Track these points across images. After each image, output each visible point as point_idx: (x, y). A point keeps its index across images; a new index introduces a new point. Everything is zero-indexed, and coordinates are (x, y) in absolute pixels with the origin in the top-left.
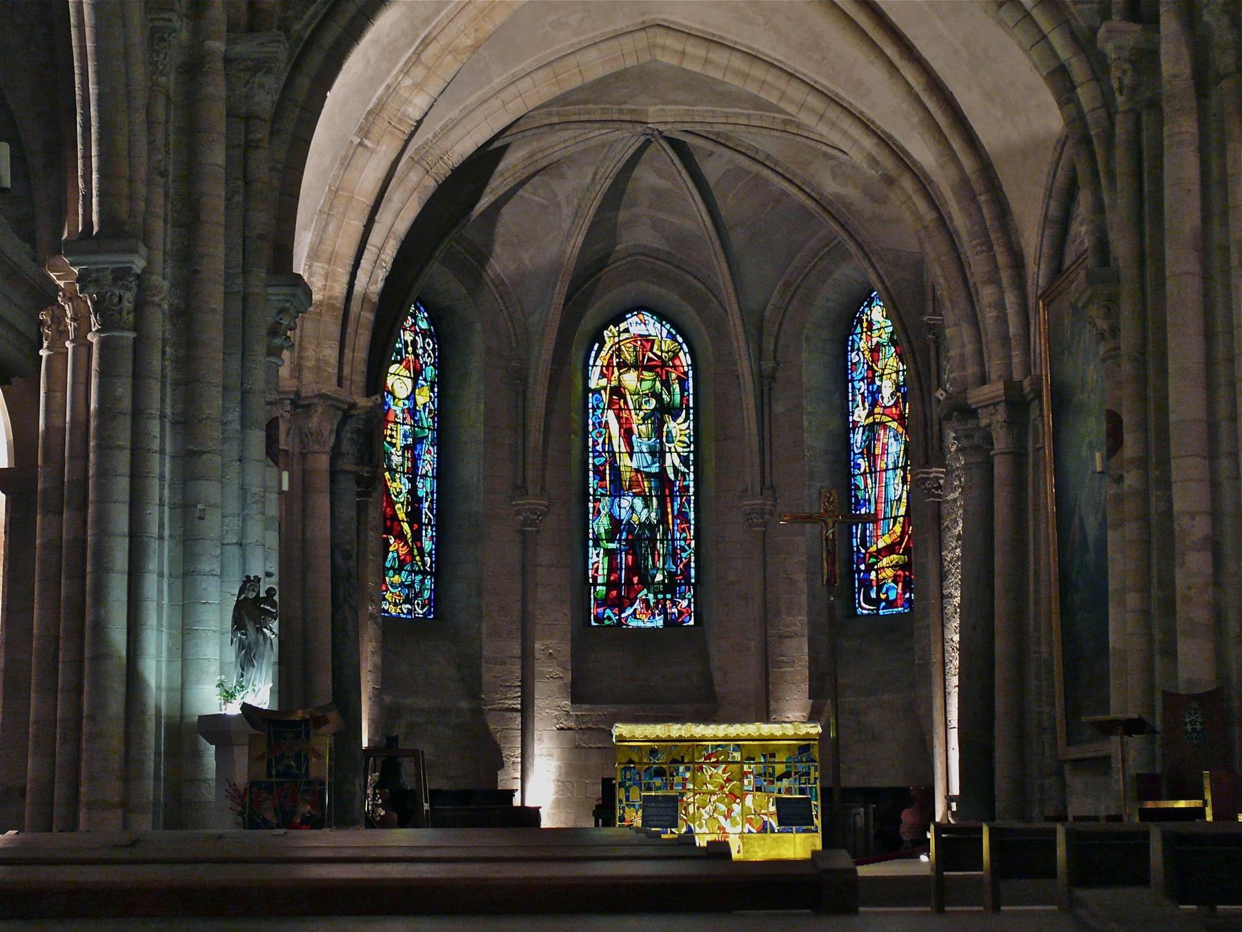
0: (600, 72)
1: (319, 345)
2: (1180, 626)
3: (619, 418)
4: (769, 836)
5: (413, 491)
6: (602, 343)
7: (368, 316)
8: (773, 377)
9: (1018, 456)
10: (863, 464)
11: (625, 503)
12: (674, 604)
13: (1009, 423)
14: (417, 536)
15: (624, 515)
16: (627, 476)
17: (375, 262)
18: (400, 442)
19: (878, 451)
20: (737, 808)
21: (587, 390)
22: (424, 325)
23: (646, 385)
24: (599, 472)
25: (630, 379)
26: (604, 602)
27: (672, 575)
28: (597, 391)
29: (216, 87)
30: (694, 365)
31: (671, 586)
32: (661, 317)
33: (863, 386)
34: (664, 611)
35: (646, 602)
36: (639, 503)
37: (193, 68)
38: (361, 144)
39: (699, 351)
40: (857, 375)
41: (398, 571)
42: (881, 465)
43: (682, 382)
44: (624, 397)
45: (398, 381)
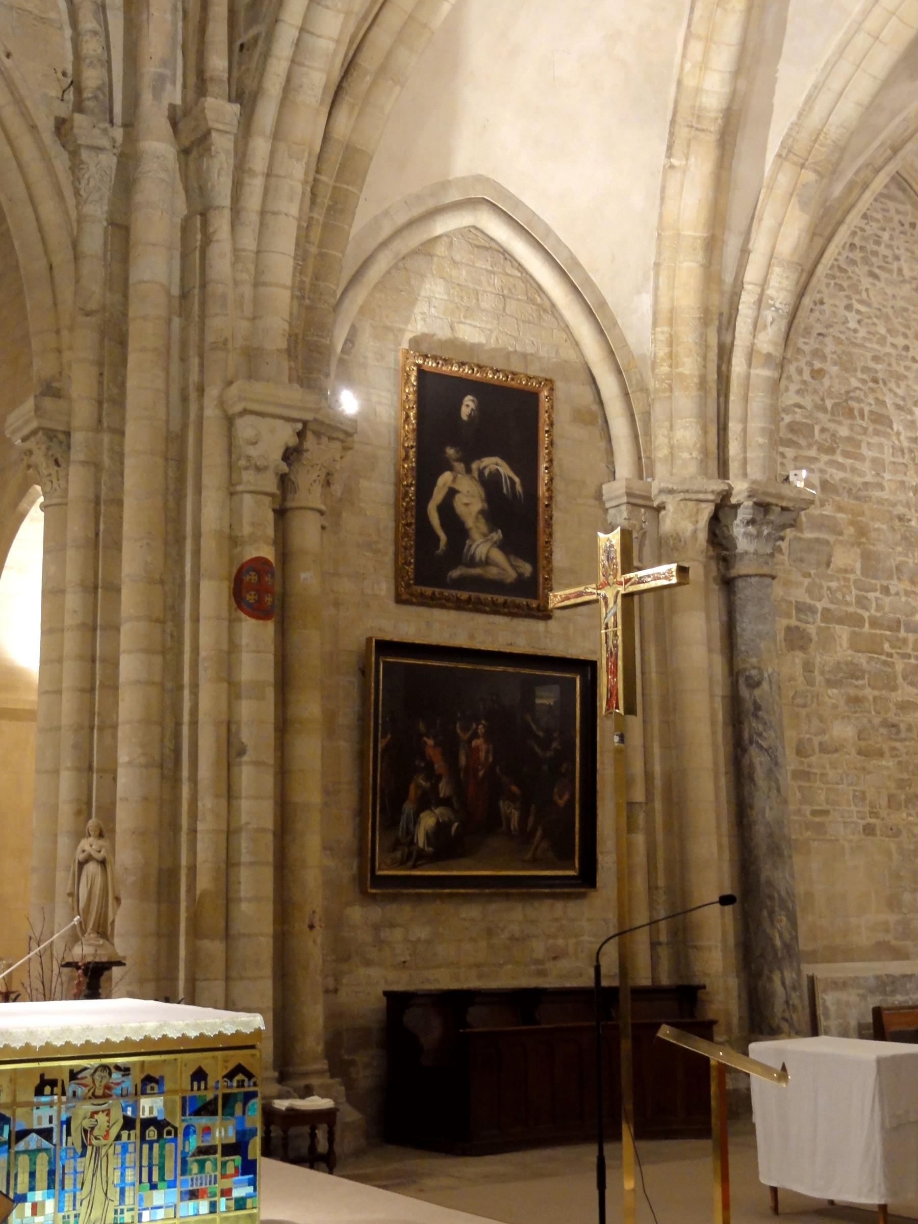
1: (671, 428)
7: (762, 373)
17: (760, 301)
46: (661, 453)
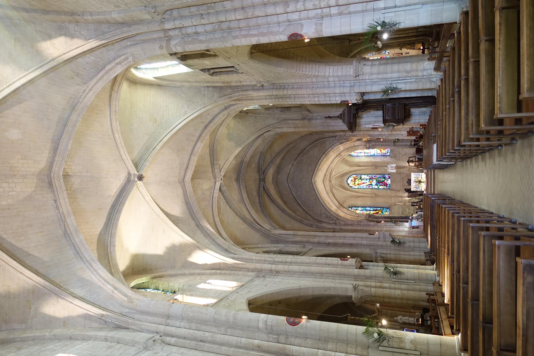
11: (373, 183)
25: (357, 183)
29: (343, 227)
31: (385, 178)
45: (358, 212)
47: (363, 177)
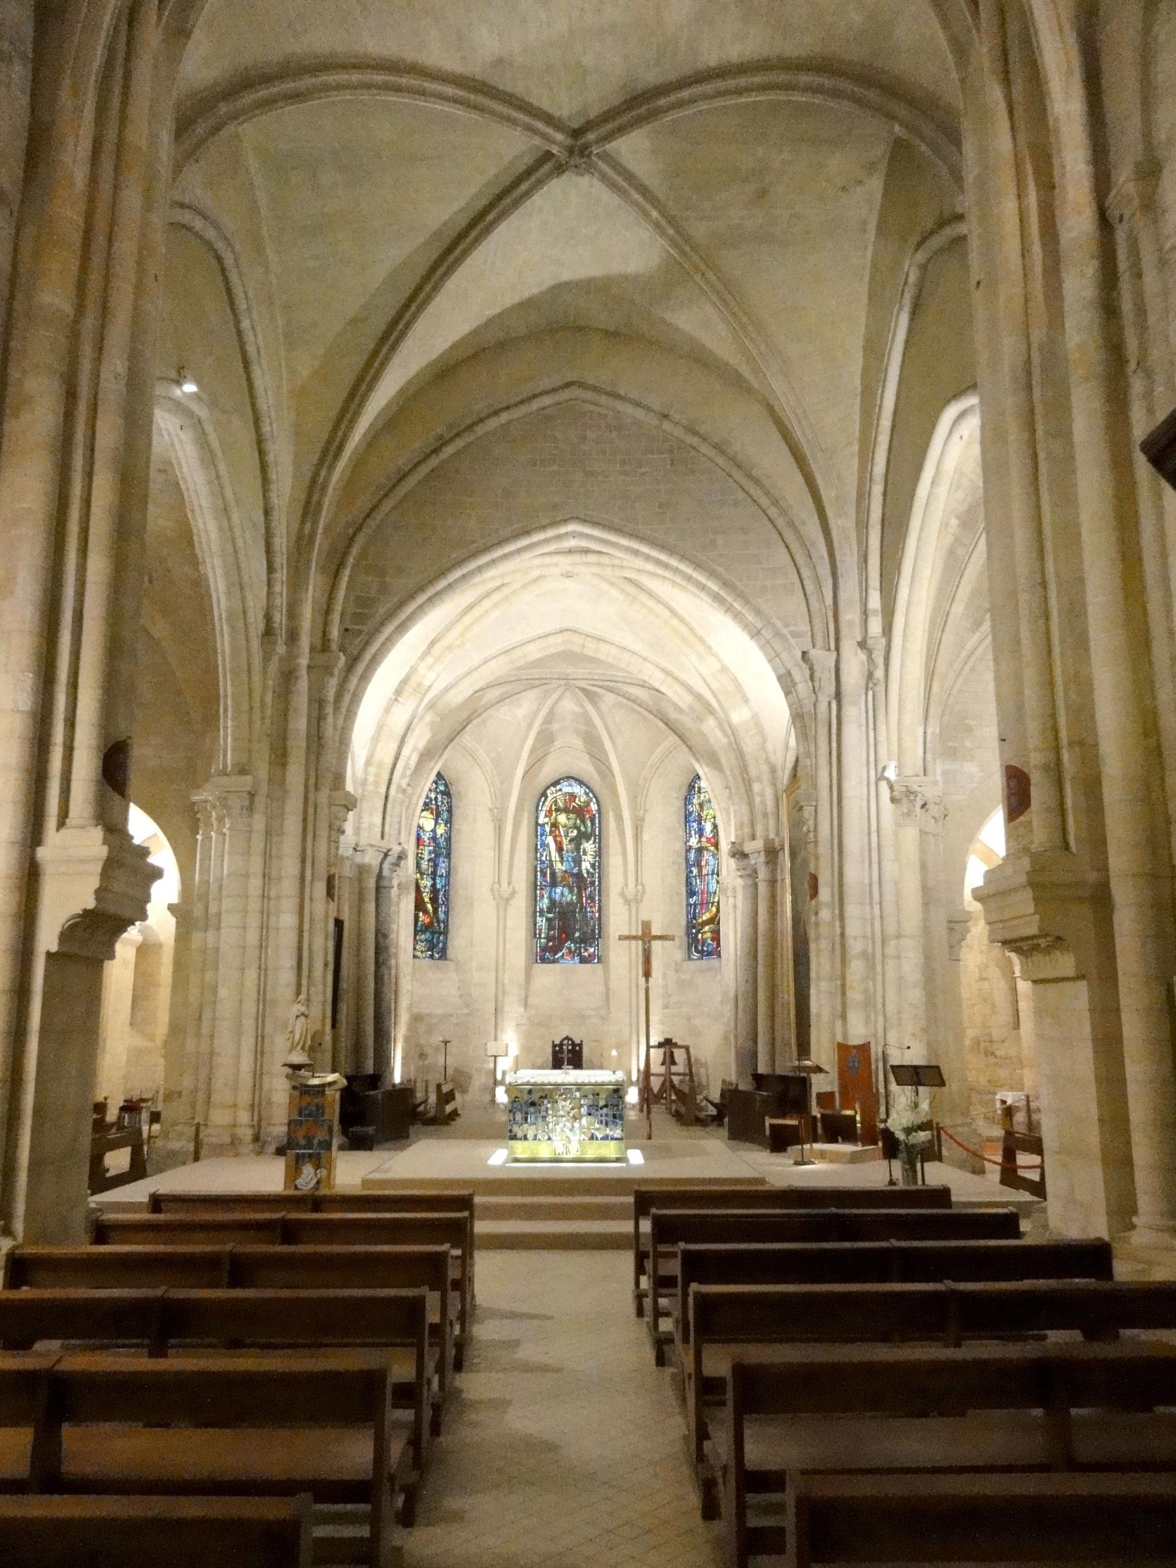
0: (537, 655)
2: (849, 1002)
3: (556, 841)
4: (594, 1142)
5: (434, 885)
6: (546, 797)
8: (643, 820)
9: (773, 882)
10: (695, 871)
11: (558, 890)
12: (586, 950)
13: (767, 863)
14: (435, 910)
15: (557, 897)
16: (559, 875)
18: (426, 857)
19: (703, 863)
20: (577, 1125)
21: (537, 824)
22: (442, 788)
23: (571, 823)
24: (544, 874)
25: (562, 818)
26: (544, 949)
27: (584, 934)
28: (543, 825)
29: (303, 684)
30: (599, 811)
32: (581, 783)
33: (695, 825)
34: (580, 954)
35: (569, 949)
36: (566, 891)
37: (288, 676)
38: (396, 699)
39: (601, 803)
40: (692, 818)
41: (423, 932)
42: (705, 871)
43: (592, 820)
44: (557, 828)
46: (364, 826)
47: (589, 846)
